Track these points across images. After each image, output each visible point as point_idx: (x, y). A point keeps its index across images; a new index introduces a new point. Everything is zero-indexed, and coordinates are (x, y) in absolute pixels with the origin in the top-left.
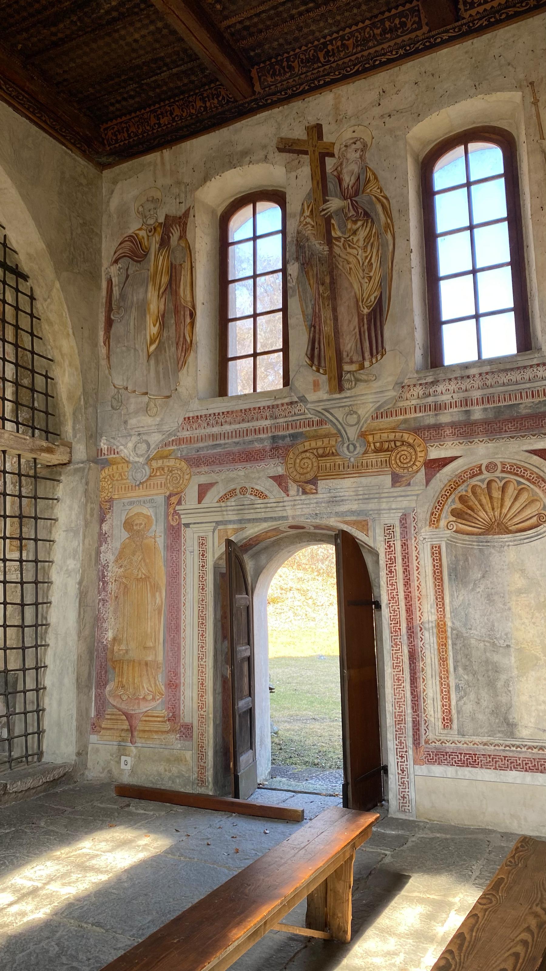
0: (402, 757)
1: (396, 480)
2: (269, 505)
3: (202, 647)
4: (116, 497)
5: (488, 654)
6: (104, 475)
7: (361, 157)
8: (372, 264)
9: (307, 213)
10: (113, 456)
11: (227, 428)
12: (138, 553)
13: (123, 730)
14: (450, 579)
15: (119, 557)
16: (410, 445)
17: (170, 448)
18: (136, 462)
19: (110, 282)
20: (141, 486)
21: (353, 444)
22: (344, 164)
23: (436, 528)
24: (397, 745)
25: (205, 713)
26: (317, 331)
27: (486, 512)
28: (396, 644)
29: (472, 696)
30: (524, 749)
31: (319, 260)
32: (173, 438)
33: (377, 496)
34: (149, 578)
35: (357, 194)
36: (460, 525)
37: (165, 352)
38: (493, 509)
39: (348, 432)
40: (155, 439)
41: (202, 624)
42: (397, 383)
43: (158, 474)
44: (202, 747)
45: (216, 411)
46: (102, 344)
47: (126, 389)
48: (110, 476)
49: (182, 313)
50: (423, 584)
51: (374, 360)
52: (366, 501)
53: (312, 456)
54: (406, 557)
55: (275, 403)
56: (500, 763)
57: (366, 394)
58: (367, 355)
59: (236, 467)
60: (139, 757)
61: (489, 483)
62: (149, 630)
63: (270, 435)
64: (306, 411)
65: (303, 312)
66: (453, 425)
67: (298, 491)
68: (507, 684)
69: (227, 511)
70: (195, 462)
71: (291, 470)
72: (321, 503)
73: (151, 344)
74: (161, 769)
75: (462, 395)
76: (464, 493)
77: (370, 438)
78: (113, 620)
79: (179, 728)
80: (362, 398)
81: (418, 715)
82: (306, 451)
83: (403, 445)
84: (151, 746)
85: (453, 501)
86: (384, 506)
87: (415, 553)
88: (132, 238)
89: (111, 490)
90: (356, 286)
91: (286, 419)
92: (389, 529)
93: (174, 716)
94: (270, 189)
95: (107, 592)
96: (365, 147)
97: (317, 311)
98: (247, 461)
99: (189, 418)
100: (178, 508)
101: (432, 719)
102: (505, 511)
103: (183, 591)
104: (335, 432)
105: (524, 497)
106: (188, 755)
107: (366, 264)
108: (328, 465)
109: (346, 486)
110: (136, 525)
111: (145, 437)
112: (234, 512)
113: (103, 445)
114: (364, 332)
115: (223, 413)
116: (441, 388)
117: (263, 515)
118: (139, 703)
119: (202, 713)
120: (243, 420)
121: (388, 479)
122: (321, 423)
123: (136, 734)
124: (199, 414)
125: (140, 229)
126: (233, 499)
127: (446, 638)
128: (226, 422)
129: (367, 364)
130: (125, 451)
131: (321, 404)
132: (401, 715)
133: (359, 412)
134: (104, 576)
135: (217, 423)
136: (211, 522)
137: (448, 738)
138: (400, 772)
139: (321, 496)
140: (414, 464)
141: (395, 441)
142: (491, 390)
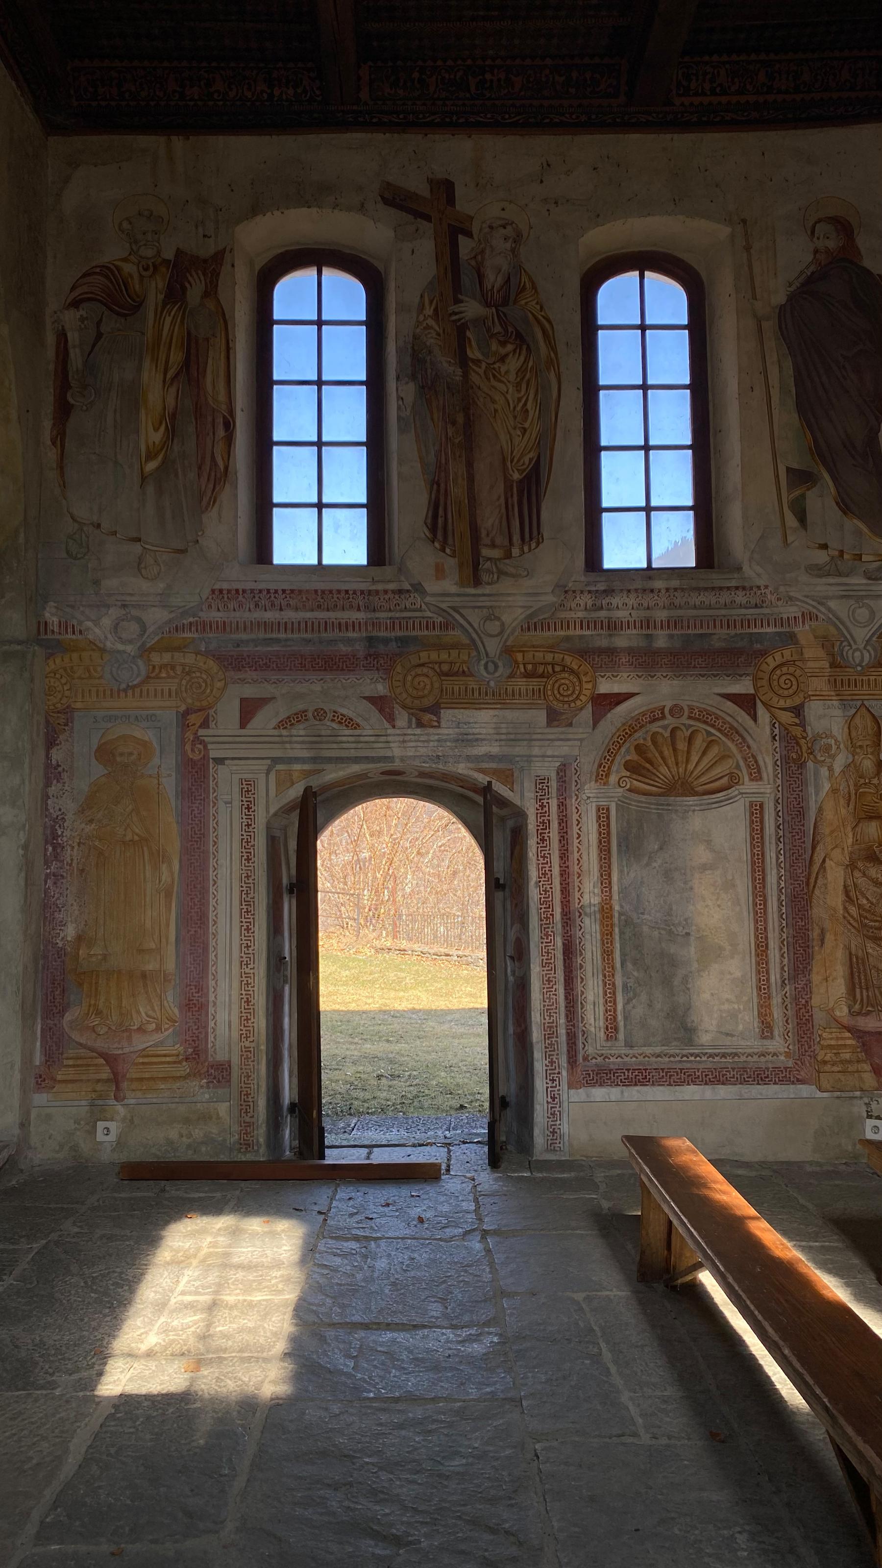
0: (553, 1080)
1: (553, 717)
2: (362, 739)
3: (248, 947)
4: (79, 705)
5: (663, 945)
6: (53, 666)
7: (513, 250)
8: (527, 411)
9: (429, 311)
10: (70, 636)
11: (290, 615)
13: (99, 1081)
14: (619, 851)
16: (572, 671)
17: (185, 635)
18: (118, 652)
19: (62, 336)
20: (130, 692)
21: (493, 662)
22: (487, 252)
23: (605, 784)
24: (546, 1066)
25: (253, 1045)
26: (442, 491)
27: (668, 768)
28: (547, 935)
29: (644, 997)
30: (704, 1058)
31: (448, 388)
32: (191, 619)
33: (527, 737)
35: (505, 302)
36: (635, 782)
37: (176, 475)
38: (677, 764)
39: (486, 644)
40: (156, 617)
41: (247, 912)
42: (557, 586)
43: (164, 675)
44: (247, 1095)
45: (272, 587)
46: (49, 443)
47: (98, 526)
48: (65, 670)
49: (210, 419)
50: (585, 857)
51: (526, 549)
52: (513, 743)
53: (431, 673)
54: (564, 822)
55: (374, 588)
56: (675, 1077)
57: (514, 594)
58: (516, 538)
59: (307, 678)
60: (132, 1121)
61: (673, 731)
62: (148, 924)
63: (364, 635)
64: (424, 606)
65: (420, 458)
66: (630, 651)
67: (410, 722)
68: (685, 980)
69: (290, 742)
70: (235, 662)
71: (398, 691)
72: (446, 741)
73: (150, 457)
74: (173, 1134)
75: (643, 614)
76: (642, 742)
77: (519, 657)
78: (75, 907)
79: (205, 1069)
80: (510, 599)
81: (573, 1026)
82: (423, 665)
83: (564, 670)
84: (155, 1100)
85: (628, 751)
86: (536, 751)
87: (575, 817)
88: (106, 271)
89: (67, 693)
90: (504, 438)
91: (390, 615)
92: (541, 783)
93: (196, 1052)
94: (348, 251)
96: (518, 238)
97: (443, 461)
98: (325, 670)
99: (221, 591)
100: (201, 732)
101: (593, 1029)
102: (691, 767)
103: (212, 862)
104: (468, 642)
105: (714, 751)
106: (223, 1108)
107: (519, 408)
108: (456, 688)
109: (483, 720)
110: (122, 754)
111: (134, 612)
112: (304, 746)
113: (51, 616)
114: (513, 506)
115: (284, 591)
116: (616, 601)
117: (353, 753)
118: (129, 1039)
119: (247, 1044)
120: (319, 607)
121: (541, 716)
122: (445, 626)
123: (125, 1085)
124: (240, 586)
125: (125, 260)
126: (301, 726)
127: (612, 925)
128: (288, 605)
129: (515, 552)
130: (97, 630)
131: (447, 599)
132: (552, 1027)
133: (503, 619)
134: (55, 836)
135: (273, 605)
136: (263, 759)
137: (613, 1052)
138: (550, 1100)
139: (446, 731)
140: (577, 698)
141: (553, 665)
142: (680, 612)
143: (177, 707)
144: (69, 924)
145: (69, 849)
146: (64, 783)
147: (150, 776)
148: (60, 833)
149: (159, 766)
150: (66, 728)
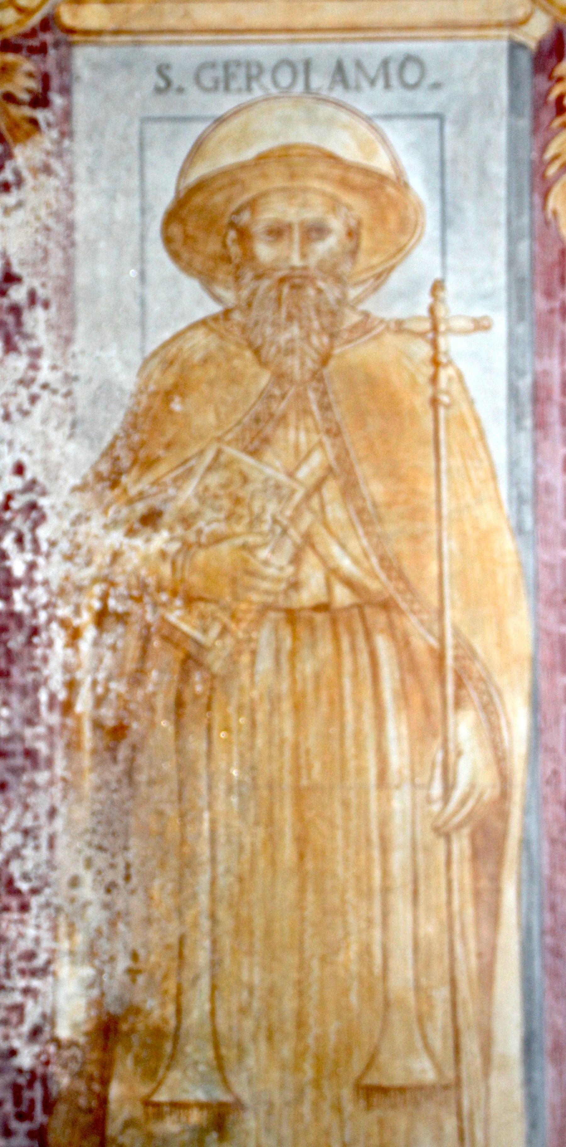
4: (92, 16)
12: (295, 435)
15: (135, 455)
34: (387, 605)
62: (402, 975)
78: (88, 891)
95: (29, 691)
143: (517, 24)
144: (64, 969)
145: (58, 635)
146: (36, 354)
147: (400, 327)
148: (18, 569)
149: (437, 287)
150: (41, 115)
